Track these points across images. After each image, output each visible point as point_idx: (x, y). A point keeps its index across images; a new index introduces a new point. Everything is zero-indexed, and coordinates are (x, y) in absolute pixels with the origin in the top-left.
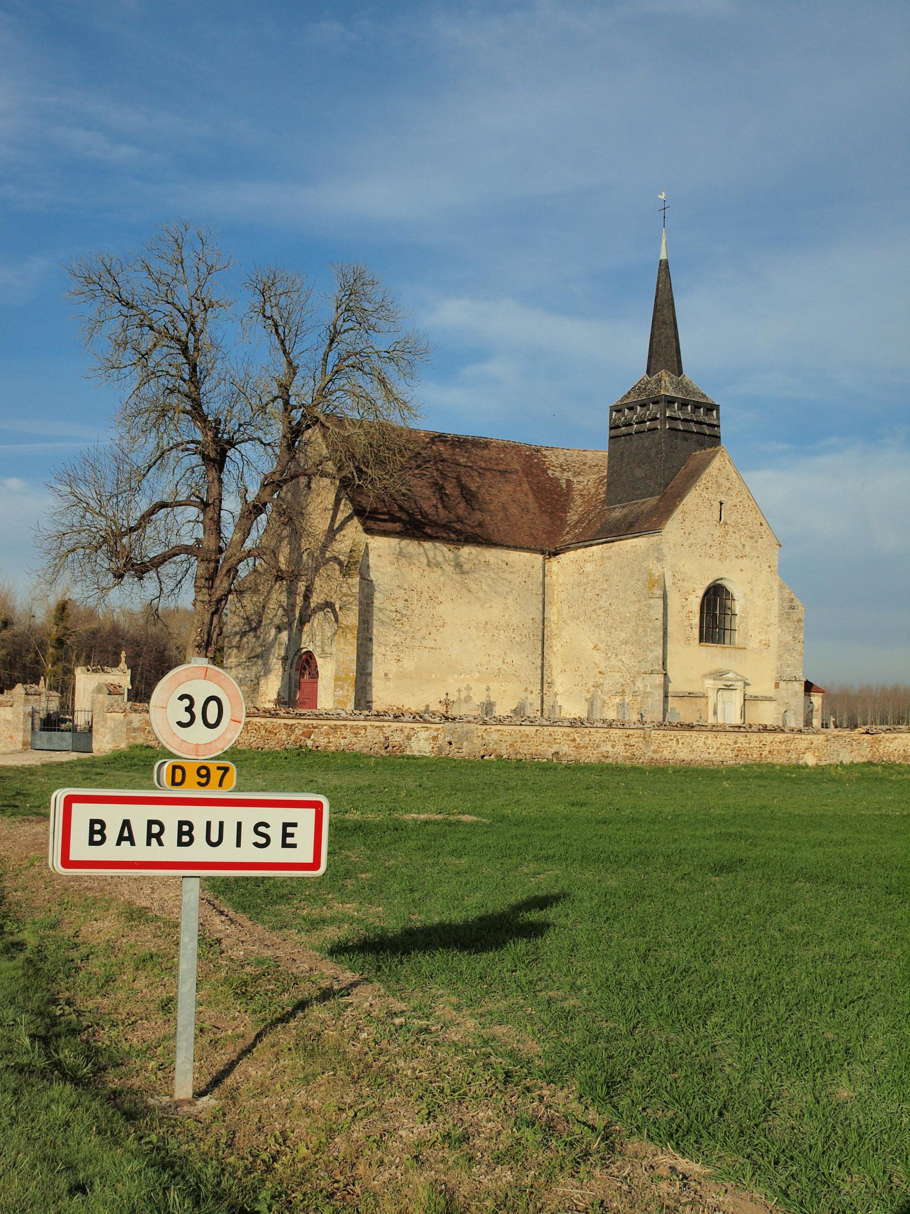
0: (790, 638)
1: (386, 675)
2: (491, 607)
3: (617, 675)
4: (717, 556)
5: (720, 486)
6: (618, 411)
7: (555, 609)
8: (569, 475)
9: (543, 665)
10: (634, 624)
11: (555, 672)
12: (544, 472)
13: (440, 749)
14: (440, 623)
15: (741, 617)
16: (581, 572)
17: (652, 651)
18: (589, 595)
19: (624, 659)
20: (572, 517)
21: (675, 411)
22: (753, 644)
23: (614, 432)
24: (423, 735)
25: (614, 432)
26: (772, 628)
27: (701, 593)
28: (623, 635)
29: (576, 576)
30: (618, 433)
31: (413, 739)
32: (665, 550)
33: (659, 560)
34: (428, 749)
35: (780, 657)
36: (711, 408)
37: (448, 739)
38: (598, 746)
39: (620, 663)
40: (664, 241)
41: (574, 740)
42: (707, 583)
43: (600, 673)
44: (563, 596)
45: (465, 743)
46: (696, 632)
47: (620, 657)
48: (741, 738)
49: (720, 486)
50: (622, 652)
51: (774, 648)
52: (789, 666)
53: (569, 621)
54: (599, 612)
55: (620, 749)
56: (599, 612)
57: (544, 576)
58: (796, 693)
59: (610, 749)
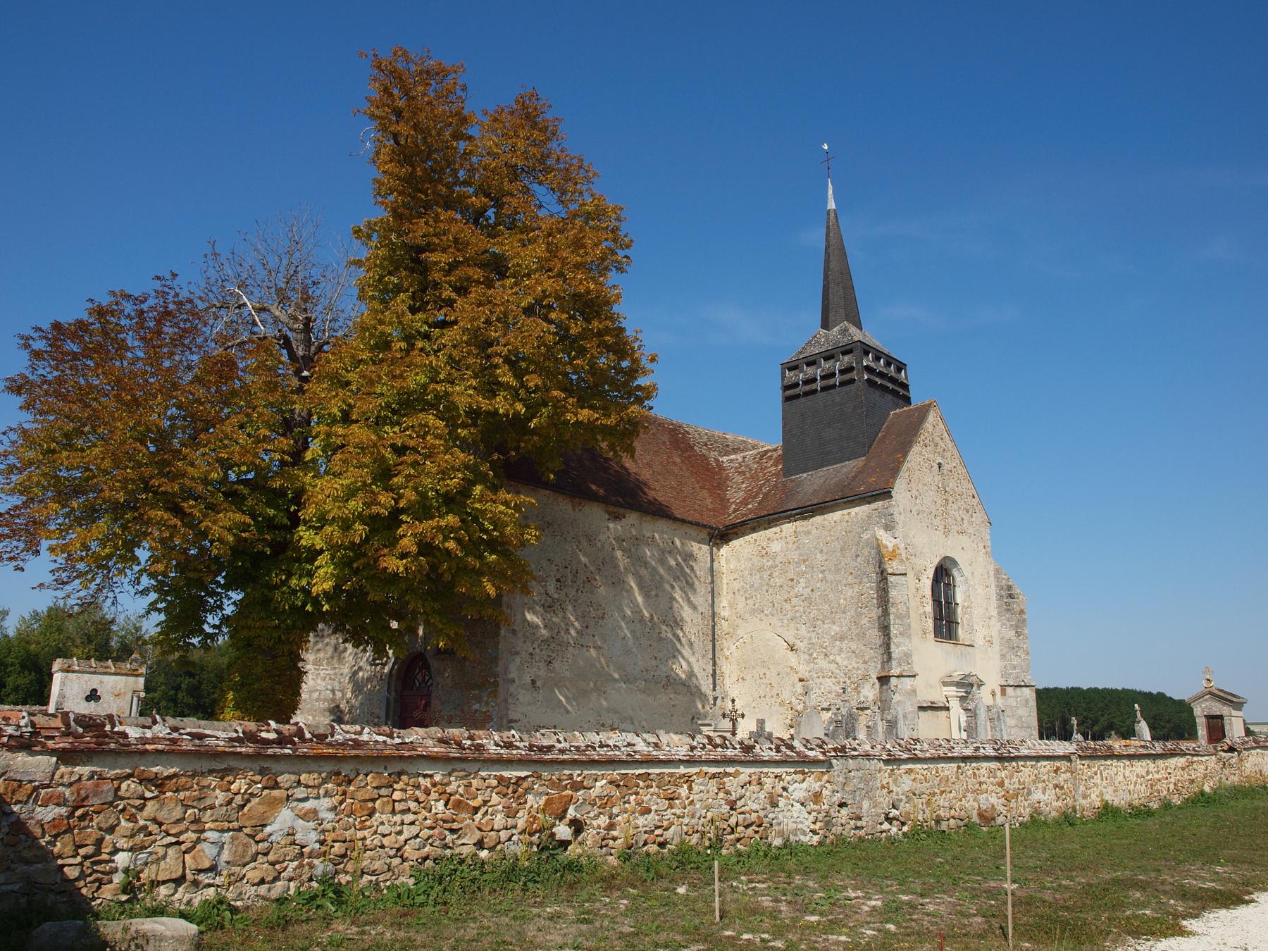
0: (1013, 633)
1: (533, 682)
2: (657, 595)
3: (829, 683)
4: (941, 527)
5: (936, 445)
6: (790, 369)
7: (725, 603)
8: (714, 454)
9: (714, 671)
10: (853, 612)
11: (728, 682)
12: (692, 448)
13: (828, 824)
14: (600, 613)
15: (963, 607)
16: (764, 553)
17: (898, 646)
18: (778, 581)
19: (838, 659)
20: (736, 494)
21: (868, 361)
22: (979, 641)
23: (789, 393)
24: (799, 790)
25: (789, 393)
26: (993, 621)
27: (931, 573)
28: (836, 628)
29: (755, 559)
30: (791, 394)
31: (782, 802)
32: (897, 517)
33: (888, 528)
34: (808, 824)
35: (1003, 656)
36: (900, 367)
37: (837, 798)
38: (1029, 793)
39: (833, 666)
40: (830, 192)
41: (1001, 784)
42: (936, 561)
43: (801, 680)
44: (736, 585)
45: (866, 804)
46: (930, 624)
47: (832, 657)
48: (1151, 765)
49: (936, 445)
50: (835, 651)
51: (996, 648)
52: (1014, 668)
53: (747, 616)
54: (795, 601)
55: (1049, 796)
56: (795, 601)
57: (712, 561)
58: (1027, 700)
59: (1042, 797)
